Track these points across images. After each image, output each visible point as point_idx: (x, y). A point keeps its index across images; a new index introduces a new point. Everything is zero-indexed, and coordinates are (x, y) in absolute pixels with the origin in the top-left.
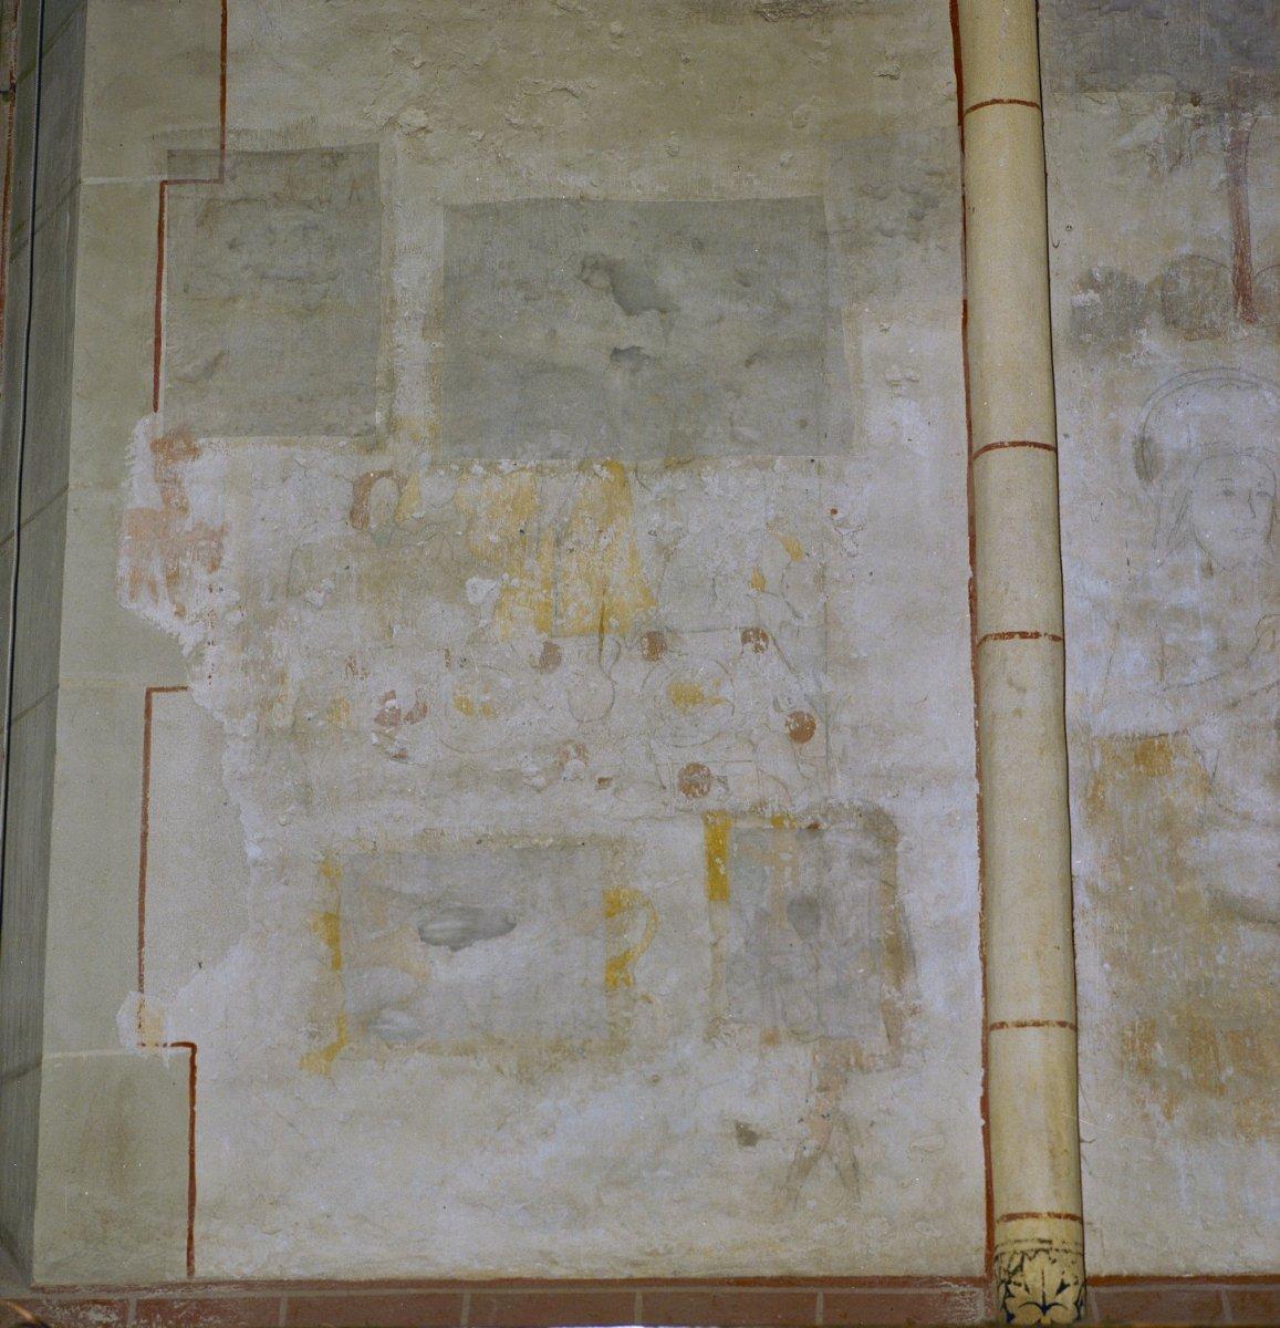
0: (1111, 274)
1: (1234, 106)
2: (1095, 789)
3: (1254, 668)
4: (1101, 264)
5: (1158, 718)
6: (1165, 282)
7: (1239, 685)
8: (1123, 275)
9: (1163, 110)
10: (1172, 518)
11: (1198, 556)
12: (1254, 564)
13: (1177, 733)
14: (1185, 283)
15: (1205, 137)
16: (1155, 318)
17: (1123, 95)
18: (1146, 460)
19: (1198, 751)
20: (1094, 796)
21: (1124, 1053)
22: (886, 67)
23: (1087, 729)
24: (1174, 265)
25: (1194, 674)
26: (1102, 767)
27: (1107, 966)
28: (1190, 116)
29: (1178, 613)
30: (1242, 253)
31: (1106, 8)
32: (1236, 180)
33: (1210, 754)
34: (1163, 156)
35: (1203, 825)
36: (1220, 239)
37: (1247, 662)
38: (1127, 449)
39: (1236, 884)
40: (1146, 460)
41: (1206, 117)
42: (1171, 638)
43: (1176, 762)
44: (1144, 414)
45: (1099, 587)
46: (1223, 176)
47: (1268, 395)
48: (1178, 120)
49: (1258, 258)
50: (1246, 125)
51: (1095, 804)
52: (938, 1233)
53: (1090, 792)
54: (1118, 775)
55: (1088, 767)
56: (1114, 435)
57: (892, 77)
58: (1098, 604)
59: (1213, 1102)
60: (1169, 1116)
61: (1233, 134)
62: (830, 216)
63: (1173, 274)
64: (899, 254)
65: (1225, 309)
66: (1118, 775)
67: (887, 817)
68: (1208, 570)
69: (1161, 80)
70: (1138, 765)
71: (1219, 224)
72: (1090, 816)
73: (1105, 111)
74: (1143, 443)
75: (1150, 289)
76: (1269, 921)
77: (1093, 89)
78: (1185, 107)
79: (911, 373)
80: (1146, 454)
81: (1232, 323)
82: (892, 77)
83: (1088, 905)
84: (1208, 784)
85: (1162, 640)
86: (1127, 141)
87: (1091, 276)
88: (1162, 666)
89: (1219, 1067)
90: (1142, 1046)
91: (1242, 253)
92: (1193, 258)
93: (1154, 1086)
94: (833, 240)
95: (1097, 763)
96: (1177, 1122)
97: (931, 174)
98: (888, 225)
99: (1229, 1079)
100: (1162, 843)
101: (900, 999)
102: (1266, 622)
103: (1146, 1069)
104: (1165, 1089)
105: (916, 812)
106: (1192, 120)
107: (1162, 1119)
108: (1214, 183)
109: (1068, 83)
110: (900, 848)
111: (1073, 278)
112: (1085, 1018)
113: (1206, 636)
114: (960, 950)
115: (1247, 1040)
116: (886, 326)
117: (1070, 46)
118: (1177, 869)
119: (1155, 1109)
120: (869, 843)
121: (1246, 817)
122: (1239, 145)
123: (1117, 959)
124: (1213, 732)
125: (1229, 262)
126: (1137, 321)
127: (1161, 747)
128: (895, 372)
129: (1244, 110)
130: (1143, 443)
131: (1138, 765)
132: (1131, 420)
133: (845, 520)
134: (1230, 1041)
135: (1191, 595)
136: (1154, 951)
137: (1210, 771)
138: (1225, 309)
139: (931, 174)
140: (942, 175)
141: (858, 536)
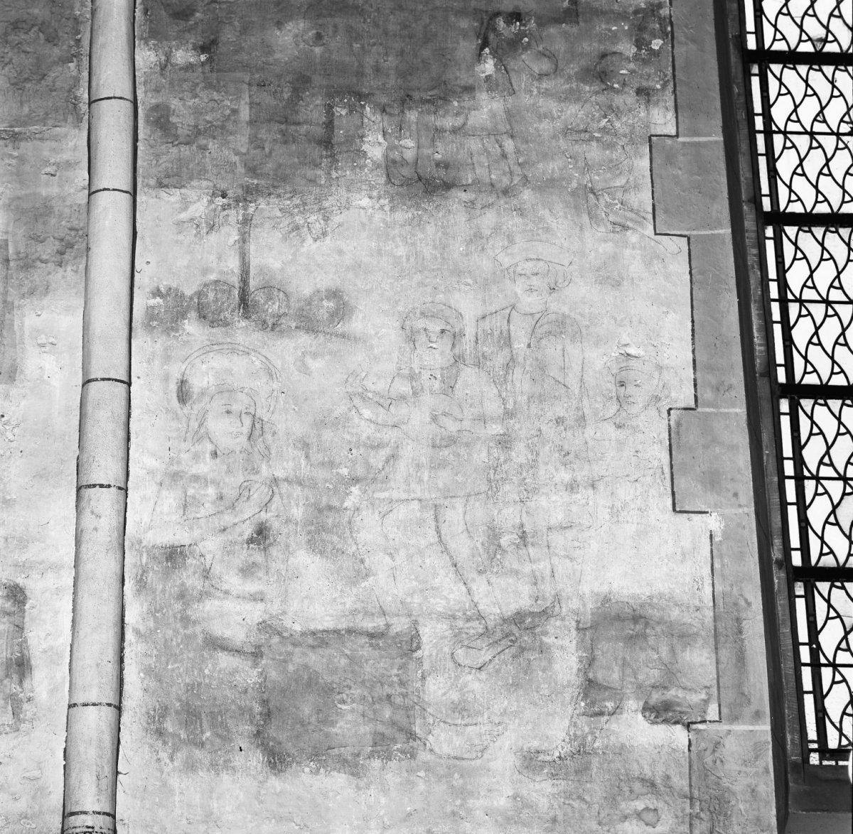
0: (170, 289)
1: (245, 200)
2: (142, 575)
3: (237, 509)
4: (165, 283)
5: (181, 537)
6: (199, 294)
7: (228, 519)
8: (177, 290)
9: (205, 200)
10: (196, 425)
11: (210, 447)
12: (241, 452)
13: (190, 545)
14: (211, 296)
15: (227, 215)
16: (193, 314)
17: (183, 191)
18: (183, 395)
19: (202, 555)
20: (141, 579)
21: (148, 724)
22: (49, 170)
23: (140, 542)
24: (206, 285)
25: (203, 512)
26: (147, 564)
27: (142, 675)
28: (221, 204)
29: (196, 478)
30: (244, 281)
31: (177, 143)
32: (244, 240)
33: (208, 557)
34: (204, 225)
35: (203, 595)
36: (233, 272)
37: (233, 507)
38: (173, 387)
39: (218, 630)
40: (183, 395)
41: (229, 205)
42: (191, 492)
43: (189, 561)
44: (184, 367)
45: (152, 463)
46: (237, 238)
47: (254, 359)
48: (213, 206)
49: (253, 283)
50: (251, 210)
51: (142, 584)
52: (34, 826)
53: (139, 577)
54: (156, 568)
55: (139, 563)
56: (166, 378)
57: (52, 175)
58: (151, 472)
59: (197, 752)
60: (172, 759)
61: (244, 215)
62: (11, 250)
63: (205, 290)
64: (49, 273)
65: (233, 311)
66: (156, 568)
67: (21, 589)
68: (215, 454)
69: (205, 183)
70: (167, 562)
71: (233, 264)
72: (138, 591)
73: (172, 199)
74: (183, 383)
75: (191, 298)
76: (236, 651)
77: (167, 186)
78: (217, 199)
79: (51, 340)
80: (184, 389)
81: (236, 319)
82: (52, 175)
83: (133, 640)
84: (206, 574)
85: (185, 493)
86: (184, 216)
87: (158, 290)
88: (185, 507)
89: (202, 732)
90: (159, 719)
91: (244, 281)
92: (217, 282)
93: (165, 743)
94: (12, 264)
95: (144, 560)
96: (176, 764)
97: (71, 229)
98: (44, 257)
99: (207, 739)
100: (178, 606)
101: (21, 692)
102: (245, 484)
103: (160, 733)
104: (170, 744)
105: (35, 586)
106: (222, 206)
107: (168, 761)
108: (231, 241)
109: (152, 182)
110: (27, 607)
111: (148, 290)
112: (127, 703)
113: (211, 491)
114: (58, 665)
115: (219, 717)
116: (39, 313)
117: (154, 162)
118: (186, 621)
119: (164, 756)
120: (9, 603)
121: (227, 592)
122: (246, 221)
123: (148, 671)
124: (211, 546)
125: (237, 285)
126: (183, 315)
127: (181, 553)
128: (42, 339)
129: (250, 202)
130: (183, 383)
131: (167, 562)
132: (176, 371)
133: (8, 421)
134: (209, 718)
135: (205, 467)
136: (169, 667)
137: (208, 567)
138: (233, 311)
139: (71, 229)
140: (77, 230)
141: (15, 430)
